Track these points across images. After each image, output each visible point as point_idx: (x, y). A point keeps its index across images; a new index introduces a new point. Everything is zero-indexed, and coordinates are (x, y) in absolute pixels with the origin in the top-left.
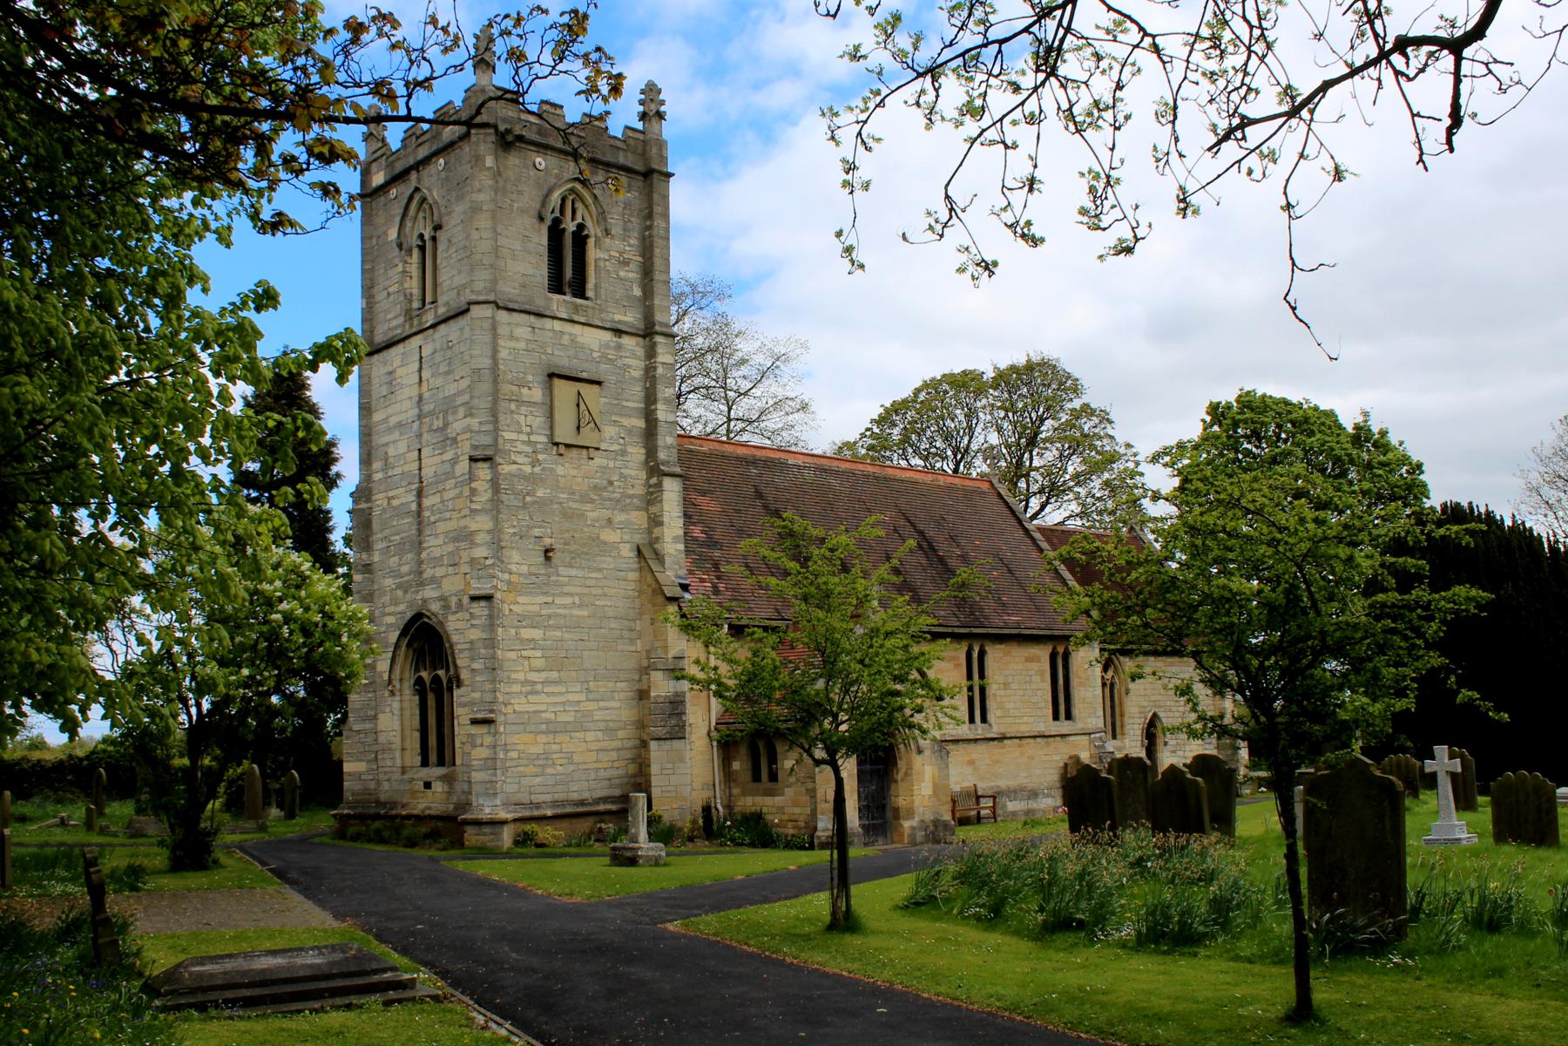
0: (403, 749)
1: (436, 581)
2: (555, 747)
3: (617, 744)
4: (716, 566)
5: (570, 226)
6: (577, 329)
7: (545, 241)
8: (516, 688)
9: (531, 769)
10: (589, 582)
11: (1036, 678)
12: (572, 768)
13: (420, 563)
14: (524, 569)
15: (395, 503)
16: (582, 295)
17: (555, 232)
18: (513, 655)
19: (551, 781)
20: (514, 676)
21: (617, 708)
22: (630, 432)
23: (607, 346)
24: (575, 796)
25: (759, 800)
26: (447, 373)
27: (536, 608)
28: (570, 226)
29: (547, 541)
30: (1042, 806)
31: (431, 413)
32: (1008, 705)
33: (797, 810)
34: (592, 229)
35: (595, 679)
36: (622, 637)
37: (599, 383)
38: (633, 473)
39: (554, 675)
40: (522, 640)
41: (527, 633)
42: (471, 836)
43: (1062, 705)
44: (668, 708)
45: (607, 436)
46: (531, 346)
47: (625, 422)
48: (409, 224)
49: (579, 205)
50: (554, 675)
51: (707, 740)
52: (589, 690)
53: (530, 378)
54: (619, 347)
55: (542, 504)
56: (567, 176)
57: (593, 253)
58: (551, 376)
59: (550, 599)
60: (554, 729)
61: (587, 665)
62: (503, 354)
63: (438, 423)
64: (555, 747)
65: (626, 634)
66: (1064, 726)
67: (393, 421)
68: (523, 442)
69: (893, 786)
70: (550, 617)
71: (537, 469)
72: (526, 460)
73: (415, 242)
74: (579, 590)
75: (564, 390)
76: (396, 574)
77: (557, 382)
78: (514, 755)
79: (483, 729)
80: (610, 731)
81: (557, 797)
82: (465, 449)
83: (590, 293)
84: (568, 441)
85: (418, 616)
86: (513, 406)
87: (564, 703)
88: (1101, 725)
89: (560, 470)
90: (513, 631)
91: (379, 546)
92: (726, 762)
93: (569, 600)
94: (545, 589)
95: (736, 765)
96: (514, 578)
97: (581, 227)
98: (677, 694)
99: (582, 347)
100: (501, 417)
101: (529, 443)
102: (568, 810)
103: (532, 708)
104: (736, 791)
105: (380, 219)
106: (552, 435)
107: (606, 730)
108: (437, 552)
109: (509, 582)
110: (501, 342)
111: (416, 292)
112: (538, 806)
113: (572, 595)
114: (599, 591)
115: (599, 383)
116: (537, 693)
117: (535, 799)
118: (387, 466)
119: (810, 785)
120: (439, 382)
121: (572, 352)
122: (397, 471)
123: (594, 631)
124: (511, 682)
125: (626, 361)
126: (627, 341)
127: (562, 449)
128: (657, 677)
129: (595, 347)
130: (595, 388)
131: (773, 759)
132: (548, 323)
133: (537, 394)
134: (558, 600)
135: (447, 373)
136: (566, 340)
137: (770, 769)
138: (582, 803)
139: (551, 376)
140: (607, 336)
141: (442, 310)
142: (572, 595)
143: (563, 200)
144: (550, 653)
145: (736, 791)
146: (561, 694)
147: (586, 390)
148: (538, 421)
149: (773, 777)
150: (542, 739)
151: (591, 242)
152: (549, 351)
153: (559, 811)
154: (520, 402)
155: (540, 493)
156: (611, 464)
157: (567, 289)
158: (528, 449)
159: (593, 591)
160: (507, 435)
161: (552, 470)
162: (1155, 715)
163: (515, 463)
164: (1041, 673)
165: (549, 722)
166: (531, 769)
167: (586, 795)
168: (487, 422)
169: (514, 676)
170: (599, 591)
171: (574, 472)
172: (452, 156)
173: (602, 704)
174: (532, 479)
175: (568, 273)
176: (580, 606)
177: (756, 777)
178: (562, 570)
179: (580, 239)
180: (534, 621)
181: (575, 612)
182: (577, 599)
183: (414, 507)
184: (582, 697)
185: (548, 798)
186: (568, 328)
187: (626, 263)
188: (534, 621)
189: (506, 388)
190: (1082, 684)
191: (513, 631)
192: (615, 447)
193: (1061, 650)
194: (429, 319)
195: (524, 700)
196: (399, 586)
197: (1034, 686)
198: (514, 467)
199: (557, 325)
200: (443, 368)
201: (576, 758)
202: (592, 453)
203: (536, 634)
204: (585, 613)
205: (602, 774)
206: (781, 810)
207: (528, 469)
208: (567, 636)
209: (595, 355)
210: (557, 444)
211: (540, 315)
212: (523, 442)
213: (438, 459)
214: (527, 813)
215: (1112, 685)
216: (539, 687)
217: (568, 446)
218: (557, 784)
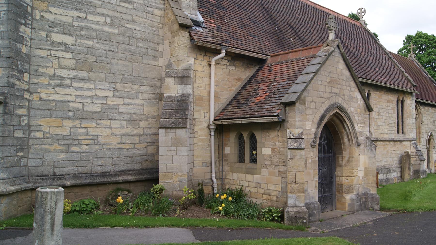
2: (81, 131)
3: (138, 131)
4: (221, 18)
8: (43, 80)
9: (56, 147)
10: (119, 9)
11: (391, 111)
12: (97, 147)
18: (43, 53)
19: (77, 157)
20: (41, 70)
21: (141, 104)
24: (99, 169)
25: (242, 176)
27: (70, 20)
30: (392, 177)
32: (380, 124)
33: (271, 187)
35: (121, 82)
36: (147, 54)
39: (84, 74)
40: (53, 43)
41: (57, 37)
43: (400, 127)
44: (174, 105)
50: (84, 74)
51: (206, 132)
52: (115, 89)
59: (83, 15)
60: (80, 116)
61: (115, 70)
64: (81, 131)
65: (150, 52)
66: (401, 137)
69: (338, 169)
70: (81, 28)
74: (110, 13)
78: (39, 135)
80: (133, 121)
81: (80, 170)
87: (92, 97)
88: (415, 137)
90: (43, 34)
92: (220, 147)
93: (101, 19)
94: (79, 6)
95: (227, 150)
98: (183, 95)
102: (89, 181)
103: (58, 98)
104: (226, 168)
107: (129, 121)
113: (104, 15)
114: (129, 18)
116: (66, 86)
117: (58, 171)
119: (283, 168)
123: (122, 46)
124: (37, 73)
128: (170, 81)
131: (254, 147)
134: (90, 17)
137: (251, 154)
138: (104, 175)
142: (104, 15)
144: (80, 57)
146: (88, 89)
149: (254, 160)
150: (68, 123)
153: (78, 182)
159: (124, 16)
162: (431, 134)
164: (393, 108)
165: (76, 111)
166: (56, 147)
167: (110, 169)
169: (41, 70)
170: (129, 18)
173: (127, 101)
176: (112, 25)
177: (241, 160)
180: (67, 29)
181: (107, 29)
182: (109, 20)
184: (110, 94)
185: (73, 170)
188: (67, 29)
190: (408, 117)
191: (43, 34)
193: (401, 98)
195: (51, 90)
197: (390, 115)
201: (101, 140)
203: (69, 40)
204: (116, 31)
205: (125, 152)
206: (258, 185)
208: (97, 45)
216: (68, 82)
218: (81, 159)
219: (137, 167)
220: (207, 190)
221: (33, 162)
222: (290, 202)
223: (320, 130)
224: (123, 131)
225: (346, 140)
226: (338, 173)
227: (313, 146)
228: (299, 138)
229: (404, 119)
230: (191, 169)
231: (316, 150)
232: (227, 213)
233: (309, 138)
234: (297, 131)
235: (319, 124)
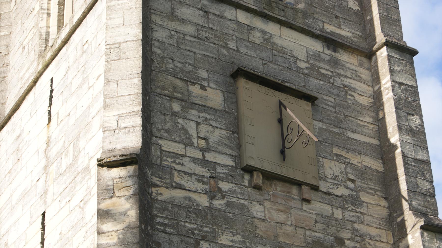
6: (272, 28)
22: (363, 173)
23: (317, 56)
38: (374, 232)
45: (328, 173)
46: (203, 34)
47: (355, 159)
53: (204, 74)
54: (335, 63)
62: (160, 34)
68: (194, 160)
71: (218, 203)
72: (199, 186)
75: (255, 100)
77: (242, 82)
84: (267, 167)
86: (176, 107)
89: (257, 210)
99: (282, 51)
100: (157, 118)
101: (204, 163)
121: (265, 54)
125: (348, 81)
126: (344, 57)
127: (258, 179)
129: (301, 54)
130: (306, 105)
133: (215, 97)
140: (317, 46)
148: (217, 135)
152: (232, 45)
154: (188, 104)
156: (338, 214)
158: (200, 170)
160: (168, 146)
161: (243, 207)
163: (180, 187)
168: (132, 114)
171: (282, 217)
186: (259, 23)
189: (165, 81)
192: (341, 191)
198: (178, 194)
199: (243, 17)
202: (307, 192)
207: (203, 201)
209: (303, 65)
210: (249, 170)
212: (194, 160)
217: (270, 177)
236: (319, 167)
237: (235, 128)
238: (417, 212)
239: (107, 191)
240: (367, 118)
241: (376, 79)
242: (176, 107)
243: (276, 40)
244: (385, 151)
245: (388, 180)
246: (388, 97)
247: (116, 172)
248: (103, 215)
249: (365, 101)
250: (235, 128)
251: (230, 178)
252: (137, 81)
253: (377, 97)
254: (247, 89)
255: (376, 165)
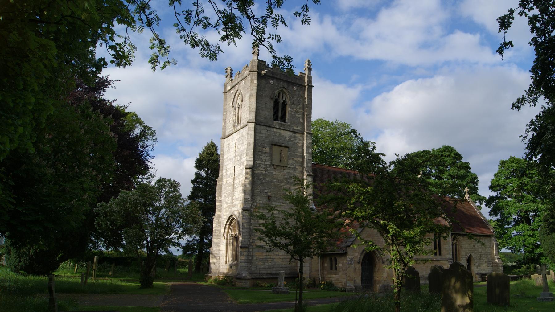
0: (226, 256)
1: (236, 205)
2: (269, 257)
5: (281, 101)
6: (281, 131)
7: (272, 105)
9: (261, 263)
13: (233, 200)
14: (261, 202)
15: (228, 182)
16: (285, 122)
17: (276, 103)
22: (297, 162)
23: (291, 136)
24: (274, 272)
26: (242, 143)
28: (281, 101)
29: (269, 194)
31: (238, 156)
34: (289, 102)
37: (288, 147)
42: (239, 284)
47: (296, 159)
48: (235, 101)
49: (284, 95)
54: (295, 137)
55: (268, 183)
56: (280, 86)
57: (288, 109)
58: (273, 145)
62: (258, 138)
63: (239, 158)
64: (269, 257)
67: (229, 158)
71: (267, 172)
73: (237, 106)
75: (276, 149)
76: (227, 203)
77: (273, 146)
78: (255, 258)
79: (245, 250)
82: (245, 166)
83: (287, 121)
85: (232, 215)
89: (274, 173)
91: (223, 195)
92: (323, 264)
95: (326, 265)
96: (258, 205)
97: (284, 101)
99: (283, 136)
100: (256, 157)
101: (265, 164)
104: (326, 273)
105: (228, 99)
106: (271, 163)
108: (237, 197)
109: (256, 206)
110: (257, 134)
111: (236, 120)
112: (262, 275)
115: (288, 147)
118: (227, 171)
120: (240, 146)
122: (229, 173)
126: (297, 135)
127: (275, 167)
130: (287, 149)
131: (336, 264)
132: (272, 129)
133: (268, 150)
135: (242, 143)
136: (278, 134)
137: (335, 266)
139: (273, 145)
140: (291, 134)
141: (242, 125)
143: (279, 93)
145: (326, 273)
147: (285, 150)
148: (268, 158)
149: (336, 269)
151: (288, 105)
154: (262, 152)
155: (267, 179)
156: (291, 172)
157: (279, 119)
158: (264, 166)
160: (258, 162)
166: (261, 263)
172: (246, 81)
174: (265, 175)
175: (280, 115)
177: (331, 269)
178: (273, 203)
179: (284, 105)
183: (232, 183)
186: (279, 131)
187: (298, 112)
194: (239, 127)
196: (228, 207)
199: (275, 130)
200: (241, 142)
201: (275, 260)
206: (338, 279)
210: (273, 165)
211: (270, 127)
213: (239, 169)
214: (258, 277)
215: (456, 245)
217: (277, 166)
219: (288, 272)
220: (317, 282)
221: (253, 269)
222: (348, 285)
223: (362, 257)
224: (283, 257)
225: (377, 260)
226: (374, 275)
227: (358, 263)
228: (351, 260)
229: (442, 246)
230: (310, 273)
231: (360, 265)
232: (324, 289)
233: (357, 260)
234: (350, 257)
235: (362, 254)
236: (288, 162)
237: (271, 156)
238: (307, 171)
239: (246, 174)
240: (300, 149)
241: (304, 140)
242: (260, 153)
243: (282, 134)
244: (303, 157)
245: (302, 163)
246: (305, 145)
247: (248, 170)
248: (246, 178)
249: (300, 145)
250: (271, 156)
251: (269, 167)
252: (252, 151)
253: (303, 144)
254: (275, 148)
255: (301, 160)
